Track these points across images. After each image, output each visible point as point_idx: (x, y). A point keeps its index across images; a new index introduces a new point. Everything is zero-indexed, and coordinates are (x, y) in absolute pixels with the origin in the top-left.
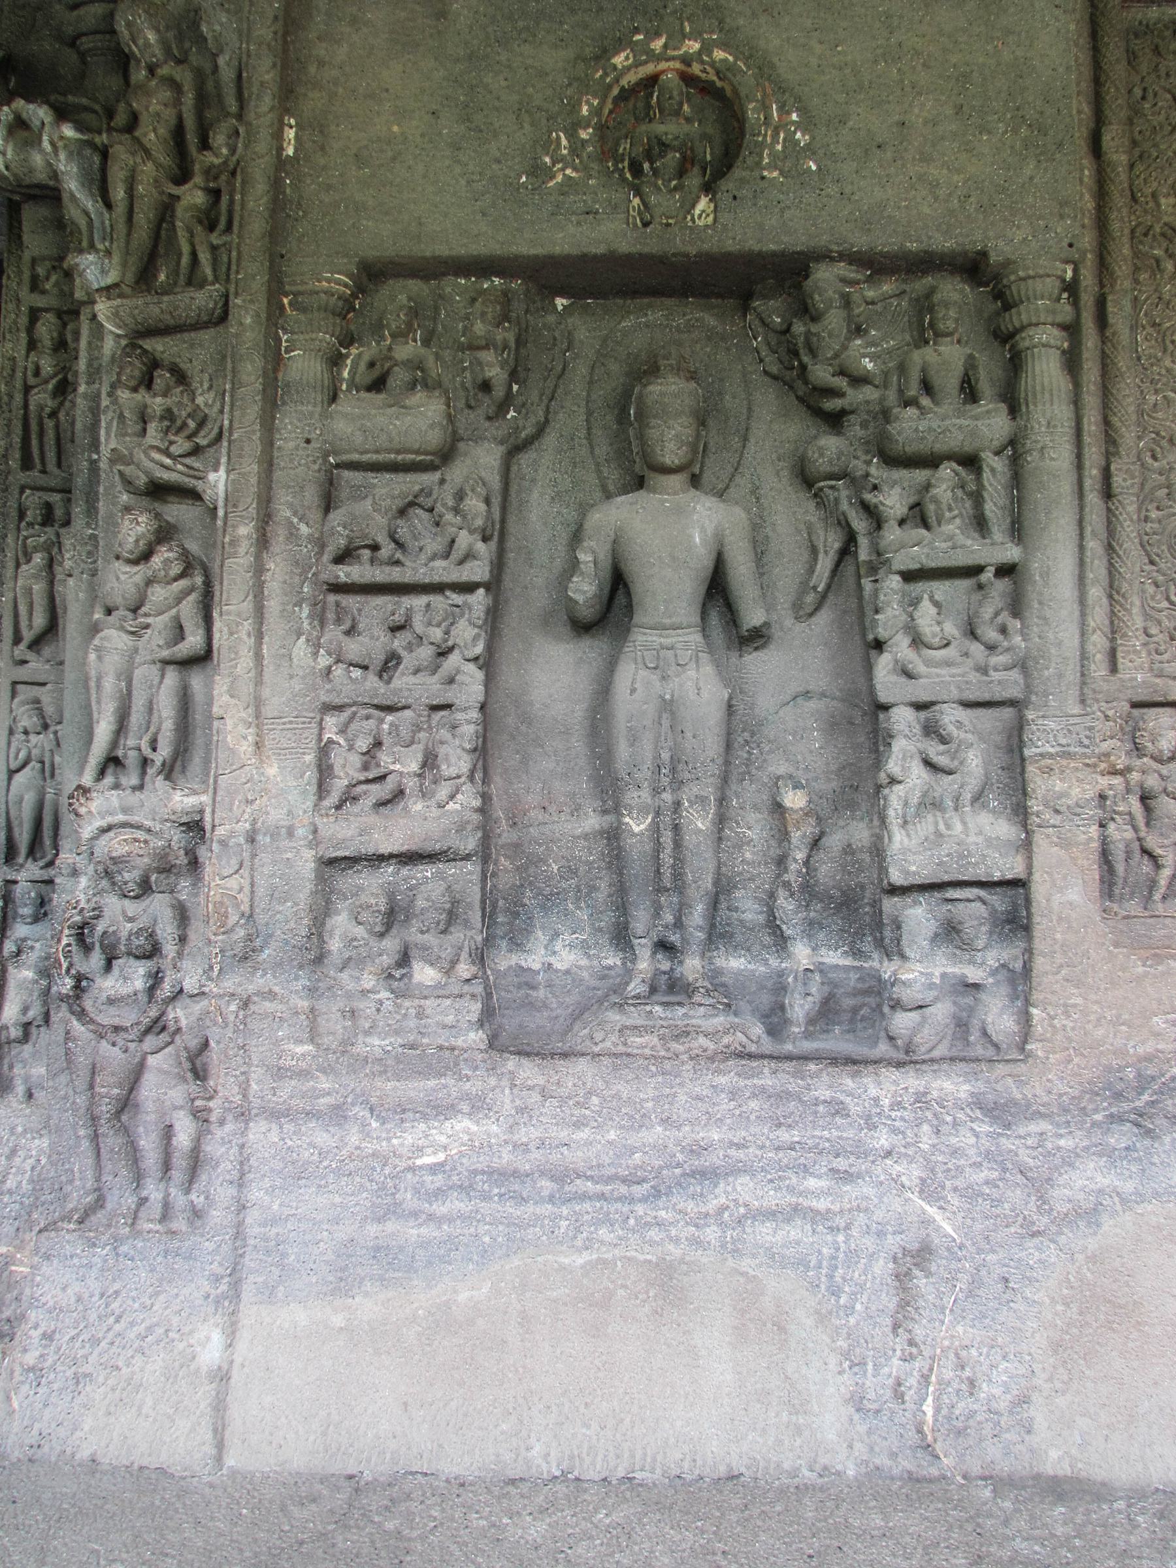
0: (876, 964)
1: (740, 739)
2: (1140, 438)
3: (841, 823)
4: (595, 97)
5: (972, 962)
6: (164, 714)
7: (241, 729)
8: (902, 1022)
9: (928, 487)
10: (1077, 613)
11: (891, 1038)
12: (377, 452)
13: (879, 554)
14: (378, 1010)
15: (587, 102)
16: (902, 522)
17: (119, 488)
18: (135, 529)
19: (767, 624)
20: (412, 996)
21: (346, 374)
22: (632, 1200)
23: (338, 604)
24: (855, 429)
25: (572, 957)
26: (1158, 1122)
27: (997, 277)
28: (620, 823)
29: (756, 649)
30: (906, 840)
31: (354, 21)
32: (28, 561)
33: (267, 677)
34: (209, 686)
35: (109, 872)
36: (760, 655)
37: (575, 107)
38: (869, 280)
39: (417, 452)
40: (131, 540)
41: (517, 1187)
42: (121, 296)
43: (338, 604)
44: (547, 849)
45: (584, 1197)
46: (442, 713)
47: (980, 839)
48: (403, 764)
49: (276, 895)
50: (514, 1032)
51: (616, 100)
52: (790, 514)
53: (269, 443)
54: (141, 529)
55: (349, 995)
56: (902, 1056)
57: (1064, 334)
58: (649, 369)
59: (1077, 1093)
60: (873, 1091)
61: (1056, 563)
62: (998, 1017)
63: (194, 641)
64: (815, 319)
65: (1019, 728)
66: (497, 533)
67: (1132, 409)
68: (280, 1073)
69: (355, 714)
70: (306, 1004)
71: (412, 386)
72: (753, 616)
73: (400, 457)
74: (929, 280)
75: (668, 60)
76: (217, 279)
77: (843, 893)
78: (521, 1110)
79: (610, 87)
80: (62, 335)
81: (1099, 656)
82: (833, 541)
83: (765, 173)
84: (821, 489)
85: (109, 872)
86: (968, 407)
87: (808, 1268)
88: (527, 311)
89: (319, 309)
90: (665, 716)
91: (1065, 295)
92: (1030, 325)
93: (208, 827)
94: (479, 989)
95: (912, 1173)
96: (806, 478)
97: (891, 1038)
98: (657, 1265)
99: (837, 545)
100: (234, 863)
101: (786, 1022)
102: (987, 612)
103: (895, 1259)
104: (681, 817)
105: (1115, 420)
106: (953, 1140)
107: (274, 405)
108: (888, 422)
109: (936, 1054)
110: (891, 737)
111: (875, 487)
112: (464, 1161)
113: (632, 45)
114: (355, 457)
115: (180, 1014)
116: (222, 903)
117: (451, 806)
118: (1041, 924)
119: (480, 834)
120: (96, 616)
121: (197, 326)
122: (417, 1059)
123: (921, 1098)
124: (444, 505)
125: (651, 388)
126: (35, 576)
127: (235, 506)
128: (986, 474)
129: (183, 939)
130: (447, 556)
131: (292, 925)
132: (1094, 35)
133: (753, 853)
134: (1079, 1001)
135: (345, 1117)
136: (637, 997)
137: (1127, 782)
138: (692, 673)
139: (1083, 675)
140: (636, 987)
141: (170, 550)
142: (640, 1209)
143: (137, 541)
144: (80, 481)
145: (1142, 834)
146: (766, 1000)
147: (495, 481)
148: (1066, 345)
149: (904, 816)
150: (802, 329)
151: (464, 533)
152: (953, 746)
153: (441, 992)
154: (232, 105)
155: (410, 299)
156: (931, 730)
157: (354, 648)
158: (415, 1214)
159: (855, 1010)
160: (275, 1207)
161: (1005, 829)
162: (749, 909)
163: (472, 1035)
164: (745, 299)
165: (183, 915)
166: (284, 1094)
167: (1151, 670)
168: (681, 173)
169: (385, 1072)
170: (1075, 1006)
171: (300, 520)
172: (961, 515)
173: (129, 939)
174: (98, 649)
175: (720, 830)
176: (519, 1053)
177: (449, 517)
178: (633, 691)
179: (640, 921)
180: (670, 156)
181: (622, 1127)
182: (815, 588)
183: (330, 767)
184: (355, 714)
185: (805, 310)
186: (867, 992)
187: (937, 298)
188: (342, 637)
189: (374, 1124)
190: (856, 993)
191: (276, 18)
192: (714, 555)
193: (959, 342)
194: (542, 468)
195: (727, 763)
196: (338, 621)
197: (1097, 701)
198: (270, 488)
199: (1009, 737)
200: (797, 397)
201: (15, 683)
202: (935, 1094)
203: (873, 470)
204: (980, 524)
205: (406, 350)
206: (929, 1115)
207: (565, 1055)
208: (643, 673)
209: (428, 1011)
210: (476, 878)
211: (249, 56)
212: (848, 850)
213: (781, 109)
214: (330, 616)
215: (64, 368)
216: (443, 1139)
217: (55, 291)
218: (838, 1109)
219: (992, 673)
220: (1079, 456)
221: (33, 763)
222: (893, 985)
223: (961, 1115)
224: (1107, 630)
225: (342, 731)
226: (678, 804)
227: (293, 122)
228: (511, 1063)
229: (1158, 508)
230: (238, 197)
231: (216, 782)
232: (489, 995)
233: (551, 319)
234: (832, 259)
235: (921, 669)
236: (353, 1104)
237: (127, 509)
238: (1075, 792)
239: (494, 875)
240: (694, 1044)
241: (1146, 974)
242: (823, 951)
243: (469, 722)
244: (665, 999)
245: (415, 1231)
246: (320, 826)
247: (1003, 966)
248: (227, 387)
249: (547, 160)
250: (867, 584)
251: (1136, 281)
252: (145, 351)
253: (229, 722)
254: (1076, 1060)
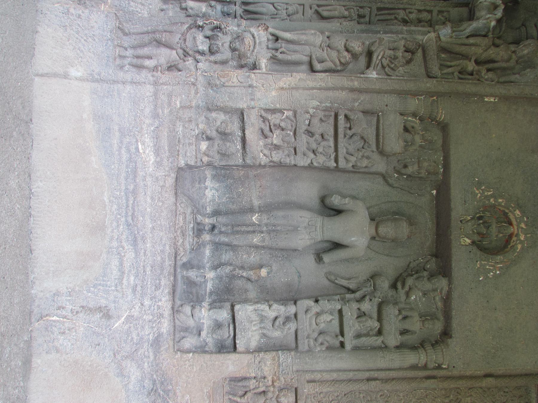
0: (207, 300)
1: (284, 254)
2: (388, 390)
3: (256, 288)
4: (505, 204)
5: (208, 333)
6: (293, 56)
7: (288, 83)
8: (187, 309)
9: (371, 318)
10: (328, 369)
11: (182, 305)
12: (383, 129)
13: (348, 301)
14: (191, 130)
15: (503, 201)
16: (359, 309)
17: (371, 41)
18: (357, 46)
19: (324, 263)
20: (196, 141)
21: (410, 118)
22: (126, 216)
23: (331, 116)
24: (391, 293)
25: (210, 196)
26: (153, 397)
27: (443, 341)
28: (256, 213)
29: (315, 259)
30: (249, 311)
32: (346, 10)
33: (306, 91)
34: (303, 72)
35: (239, 37)
36: (313, 261)
37: (501, 197)
38: (442, 298)
39: (383, 143)
40: (353, 45)
41: (131, 177)
42: (436, 41)
43: (331, 116)
44: (247, 188)
45: (127, 200)
46: (293, 152)
47: (250, 336)
48: (276, 138)
49: (231, 95)
50: (184, 177)
51: (504, 211)
52: (361, 271)
53: (386, 92)
54: (356, 48)
55: (196, 120)
56: (176, 309)
57: (423, 365)
58: (411, 222)
59: (163, 369)
60: (163, 299)
61: (344, 362)
62: (189, 342)
63: (318, 66)
64: (428, 279)
65: (289, 350)
66: (355, 170)
67: (398, 388)
68: (170, 96)
69: (293, 121)
70: (194, 105)
71: (406, 141)
72: (327, 258)
74: (442, 318)
75: (518, 229)
76: (442, 74)
77: (232, 289)
78: (157, 178)
79: (508, 209)
80: (423, 21)
81: (313, 376)
82: (352, 286)
83: (479, 262)
84: (370, 281)
85: (239, 37)
86: (398, 332)
87: (103, 277)
88: (431, 181)
89: (432, 109)
90: (292, 228)
91: (437, 365)
92: (427, 353)
93: (254, 71)
94: (199, 164)
95: (136, 313)
96: (373, 276)
97: (182, 305)
98: (104, 225)
99: (351, 287)
100: (242, 80)
101: (187, 270)
102: (328, 338)
103: (106, 307)
104: (258, 233)
105: (394, 382)
106: (147, 327)
107: (399, 94)
108: (393, 304)
109: (177, 321)
110: (285, 306)
111: (371, 300)
112: (140, 159)
113: (523, 217)
114: (381, 122)
115: (190, 61)
116: (228, 76)
117: (261, 155)
118: (221, 357)
119: (252, 164)
120: (327, 33)
121: (426, 67)
122: (175, 144)
123: (161, 316)
124: (365, 152)
125: (405, 223)
127: (365, 80)
128: (375, 338)
129: (216, 63)
130: (347, 153)
131: (221, 100)
132: (526, 375)
133: (245, 258)
134: (195, 370)
135: (155, 118)
136: (196, 218)
137: (270, 386)
138: (307, 237)
139: (307, 371)
140: (199, 218)
141: (349, 58)
142: (123, 219)
143: (352, 47)
144: (373, 27)
145: (252, 391)
146: (195, 262)
147: (373, 170)
148: (420, 365)
149: (258, 310)
150: (425, 275)
151: (355, 159)
152: (282, 327)
153: (198, 151)
154: (502, 80)
155: (435, 141)
156: (287, 319)
157: (316, 121)
158: (121, 142)
159: (191, 293)
161: (253, 344)
162: (226, 257)
163: (183, 162)
164: (436, 256)
165: (224, 63)
167: (308, 394)
168: (479, 234)
169: (170, 132)
170: (193, 368)
171: (360, 103)
172: (361, 329)
173: (216, 44)
174: (315, 34)
175: (253, 247)
176: (177, 178)
177: (361, 154)
178: (301, 217)
179: (222, 219)
180: (485, 230)
181: (151, 213)
182: (336, 279)
183: (275, 113)
184: (293, 121)
185: (432, 276)
186: (198, 297)
187: (436, 321)
188: (319, 117)
189: (152, 128)
190: (197, 293)
191: (532, 95)
192: (348, 245)
193: (421, 329)
194: (379, 185)
195: (276, 249)
196: (325, 116)
197: (298, 376)
198: (371, 93)
199: (285, 346)
200: (402, 273)
201: (304, 5)
202: (163, 320)
203: (377, 299)
204: (358, 336)
205: (418, 139)
206: (156, 318)
207: (176, 194)
208: (307, 220)
209: (191, 147)
210: (237, 163)
211: (519, 85)
212: (246, 291)
213: (501, 268)
214: (327, 113)
216: (147, 152)
218: (157, 287)
219: (307, 340)
220: (382, 370)
221: (276, 11)
222: (200, 306)
223: (155, 329)
224: (322, 379)
225: (287, 117)
226: (262, 232)
227: (496, 100)
228: (173, 175)
229: (364, 397)
230: (470, 81)
231: (270, 74)
232: (197, 168)
233: (429, 189)
234: (449, 285)
235: (309, 316)
236: (159, 121)
237: (363, 44)
238: (266, 368)
239: (238, 169)
240: (180, 238)
241: (204, 393)
242: (212, 282)
243: (290, 161)
244: (195, 228)
245: (115, 142)
246: (255, 110)
247: (207, 344)
248: (405, 78)
249: (483, 188)
250: (338, 297)
251: (442, 389)
252: (417, 50)
253: (290, 79)
254: (174, 369)
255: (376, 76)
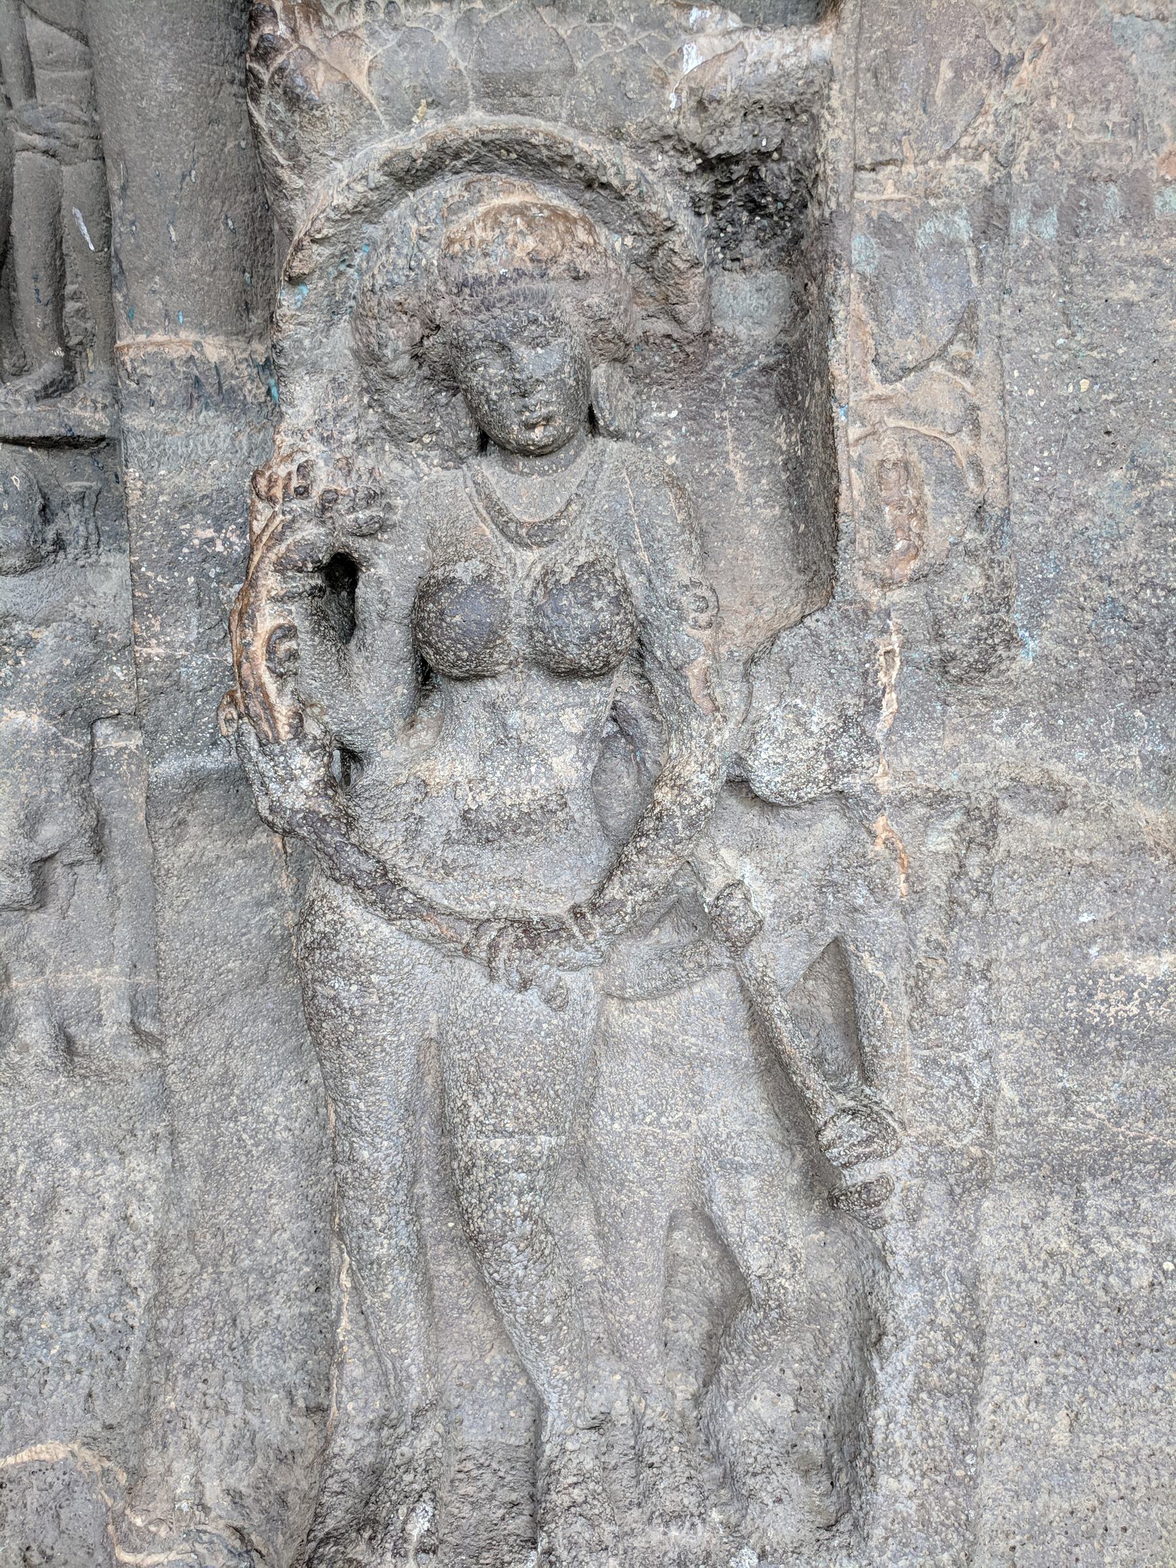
115: (740, 868)
131: (1134, 548)
160: (1061, 1437)
166: (1096, 1108)
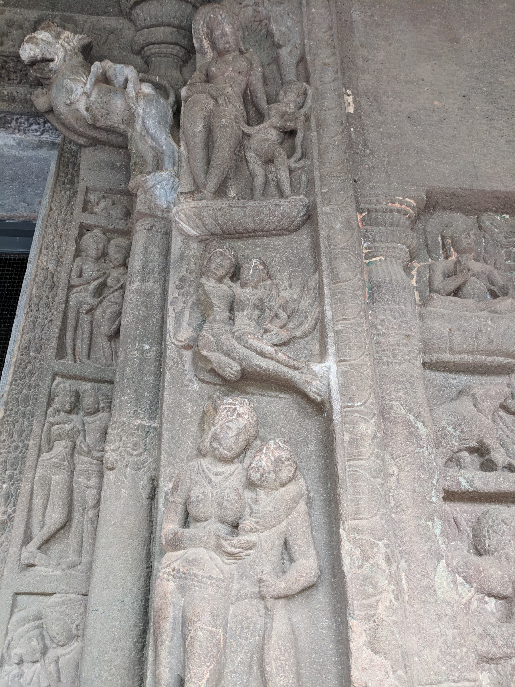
12: (472, 353)
31: (386, 38)
32: (51, 449)
40: (232, 434)
54: (242, 422)
73: (490, 359)
114: (447, 357)
126: (57, 466)
143: (237, 436)
201: (17, 594)
215: (105, 273)
217: (104, 213)
255: (331, 362)
